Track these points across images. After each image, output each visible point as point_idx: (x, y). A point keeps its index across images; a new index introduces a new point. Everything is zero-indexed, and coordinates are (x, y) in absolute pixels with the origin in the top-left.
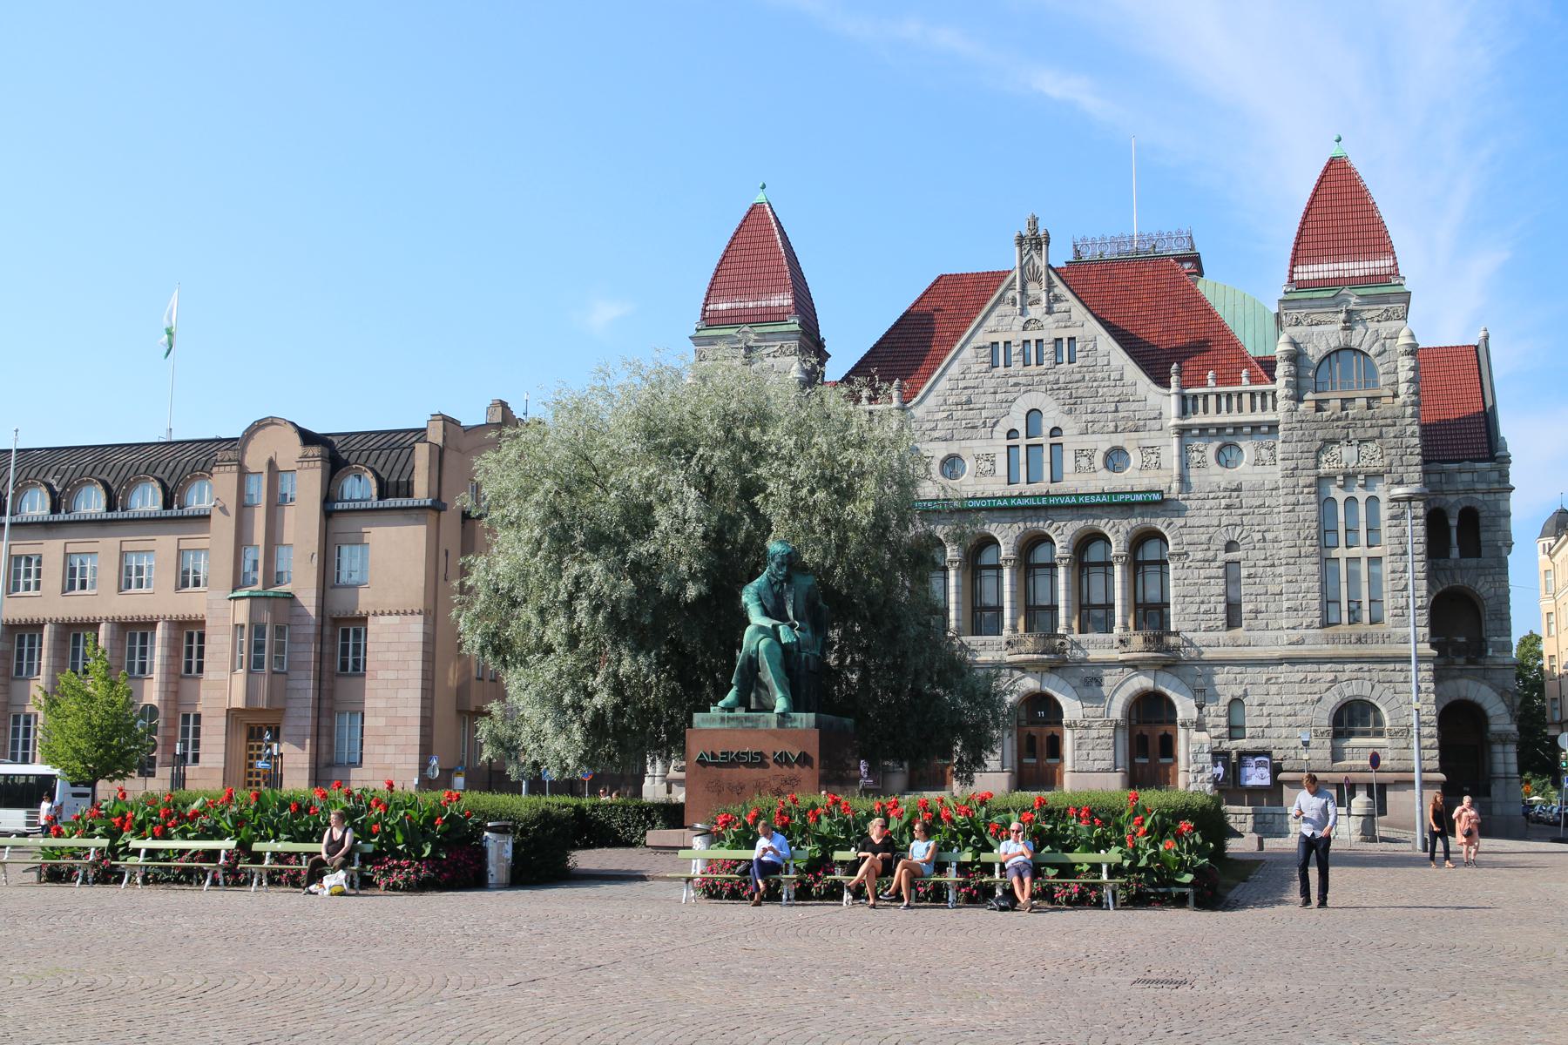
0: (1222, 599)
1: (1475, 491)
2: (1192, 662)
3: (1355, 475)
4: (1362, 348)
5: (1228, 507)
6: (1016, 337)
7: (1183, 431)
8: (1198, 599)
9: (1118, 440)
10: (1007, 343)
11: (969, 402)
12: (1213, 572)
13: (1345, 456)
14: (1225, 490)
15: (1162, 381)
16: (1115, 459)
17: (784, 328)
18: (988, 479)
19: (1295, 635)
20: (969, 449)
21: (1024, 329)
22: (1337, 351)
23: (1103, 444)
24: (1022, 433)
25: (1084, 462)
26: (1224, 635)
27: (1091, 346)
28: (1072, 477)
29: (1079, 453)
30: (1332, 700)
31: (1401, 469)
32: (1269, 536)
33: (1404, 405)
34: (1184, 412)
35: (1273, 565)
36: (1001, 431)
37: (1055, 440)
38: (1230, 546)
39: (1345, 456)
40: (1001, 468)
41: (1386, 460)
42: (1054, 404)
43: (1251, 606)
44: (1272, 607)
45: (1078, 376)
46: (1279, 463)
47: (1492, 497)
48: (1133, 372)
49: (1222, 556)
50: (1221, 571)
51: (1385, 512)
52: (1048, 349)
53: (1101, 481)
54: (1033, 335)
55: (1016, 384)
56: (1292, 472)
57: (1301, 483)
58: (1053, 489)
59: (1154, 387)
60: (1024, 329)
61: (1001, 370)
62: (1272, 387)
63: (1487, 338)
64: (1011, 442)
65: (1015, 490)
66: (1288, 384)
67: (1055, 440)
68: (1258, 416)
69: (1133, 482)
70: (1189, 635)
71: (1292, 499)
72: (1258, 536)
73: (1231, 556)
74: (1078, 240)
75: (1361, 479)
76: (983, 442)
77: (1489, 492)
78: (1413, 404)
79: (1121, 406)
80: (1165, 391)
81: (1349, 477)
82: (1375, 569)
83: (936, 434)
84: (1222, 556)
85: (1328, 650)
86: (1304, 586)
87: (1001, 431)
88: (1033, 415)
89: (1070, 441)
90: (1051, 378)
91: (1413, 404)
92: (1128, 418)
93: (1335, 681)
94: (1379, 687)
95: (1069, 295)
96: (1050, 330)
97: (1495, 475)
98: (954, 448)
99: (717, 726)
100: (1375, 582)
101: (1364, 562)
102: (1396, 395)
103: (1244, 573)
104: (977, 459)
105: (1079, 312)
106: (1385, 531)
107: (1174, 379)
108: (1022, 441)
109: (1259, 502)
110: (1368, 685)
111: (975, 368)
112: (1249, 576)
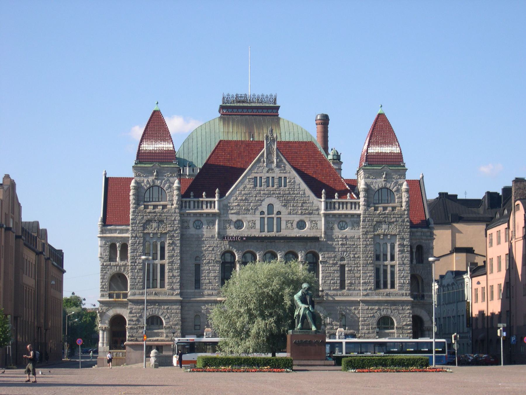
0: (339, 278)
1: (422, 239)
2: (328, 302)
3: (387, 235)
4: (391, 188)
5: (342, 244)
6: (264, 175)
7: (326, 215)
8: (330, 278)
9: (303, 217)
10: (261, 178)
11: (246, 199)
12: (335, 268)
13: (383, 229)
14: (341, 238)
15: (319, 196)
16: (301, 225)
17: (173, 166)
18: (253, 230)
19: (365, 293)
20: (246, 219)
21: (268, 172)
22: (381, 189)
23: (297, 218)
24: (266, 213)
25: (289, 225)
26: (339, 292)
27: (293, 181)
28: (284, 231)
29: (287, 222)
30: (378, 315)
31: (403, 234)
32: (356, 256)
33: (405, 210)
34: (326, 209)
35: (357, 267)
36: (258, 213)
37: (279, 216)
38: (342, 259)
39: (383, 229)
40: (258, 226)
41: (398, 230)
42: (278, 202)
43: (349, 281)
44: (357, 281)
45: (287, 192)
46: (361, 230)
47: (427, 242)
48: (309, 192)
49: (339, 263)
50: (339, 268)
51: (397, 249)
52: (276, 181)
53: (296, 233)
54: (270, 175)
55: (264, 194)
56: (366, 233)
57: (368, 237)
58: (277, 234)
59: (315, 198)
60: (268, 172)
61: (258, 188)
62: (358, 201)
63: (423, 177)
64: (262, 216)
65: (263, 235)
66: (365, 201)
67: (279, 216)
68: (353, 212)
69: (307, 233)
70: (327, 291)
71: (365, 243)
72: (352, 256)
73: (342, 263)
74: (226, 94)
75: (389, 237)
76: (251, 216)
77: (427, 240)
78: (407, 210)
79: (304, 205)
80: (320, 199)
81: (385, 235)
82: (393, 269)
83: (233, 212)
84: (339, 263)
85: (376, 298)
86: (368, 275)
87: (258, 213)
88: (270, 207)
89: (284, 217)
90: (278, 192)
91: (407, 210)
92: (306, 209)
93: (379, 309)
94: (393, 312)
95: (284, 161)
96: (277, 173)
97: (429, 234)
98: (240, 217)
99: (298, 333)
100: (393, 273)
101: (389, 267)
102: (402, 206)
103: (347, 269)
104: (249, 222)
105: (288, 167)
106: (397, 256)
107: (323, 196)
108: (266, 216)
109: (353, 243)
110: (390, 311)
111: (248, 186)
112: (349, 270)
